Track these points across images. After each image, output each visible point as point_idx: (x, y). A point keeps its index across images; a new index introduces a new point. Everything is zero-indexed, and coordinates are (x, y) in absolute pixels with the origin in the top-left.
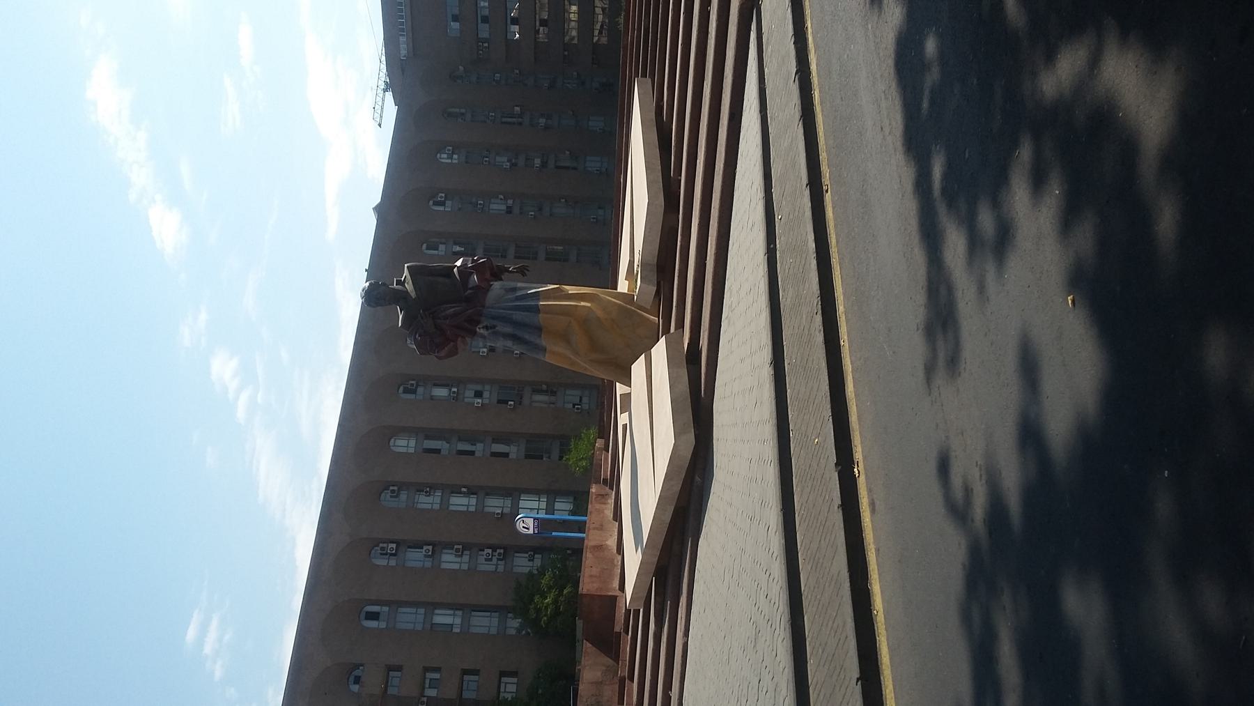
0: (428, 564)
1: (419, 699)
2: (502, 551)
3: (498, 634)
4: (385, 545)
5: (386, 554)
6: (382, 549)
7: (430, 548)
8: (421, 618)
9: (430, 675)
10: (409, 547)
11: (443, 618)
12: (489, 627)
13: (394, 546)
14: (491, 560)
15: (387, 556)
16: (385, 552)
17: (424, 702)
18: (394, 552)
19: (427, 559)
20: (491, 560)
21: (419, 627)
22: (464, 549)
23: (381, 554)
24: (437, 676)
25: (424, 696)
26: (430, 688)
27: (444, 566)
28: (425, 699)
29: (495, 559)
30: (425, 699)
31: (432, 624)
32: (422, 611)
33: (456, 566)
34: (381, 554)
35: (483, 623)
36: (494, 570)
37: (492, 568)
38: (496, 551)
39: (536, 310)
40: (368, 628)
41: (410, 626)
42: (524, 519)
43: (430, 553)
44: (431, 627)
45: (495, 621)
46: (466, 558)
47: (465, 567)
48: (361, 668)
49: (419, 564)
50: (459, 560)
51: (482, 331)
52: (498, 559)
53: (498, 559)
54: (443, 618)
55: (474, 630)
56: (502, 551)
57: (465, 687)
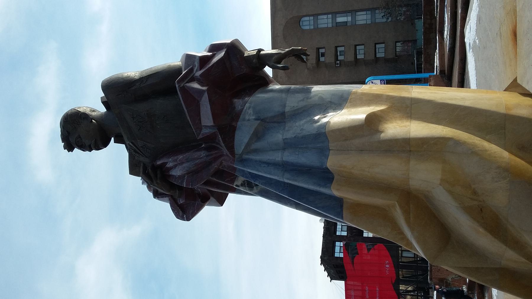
1: (336, 63)
3: (372, 23)
8: (330, 21)
11: (341, 19)
12: (366, 20)
17: (338, 63)
21: (330, 25)
24: (342, 49)
25: (338, 60)
26: (340, 55)
28: (338, 62)
30: (338, 62)
31: (336, 23)
32: (330, 16)
35: (363, 18)
40: (305, 30)
41: (326, 26)
42: (372, 81)
45: (369, 16)
54: (341, 19)
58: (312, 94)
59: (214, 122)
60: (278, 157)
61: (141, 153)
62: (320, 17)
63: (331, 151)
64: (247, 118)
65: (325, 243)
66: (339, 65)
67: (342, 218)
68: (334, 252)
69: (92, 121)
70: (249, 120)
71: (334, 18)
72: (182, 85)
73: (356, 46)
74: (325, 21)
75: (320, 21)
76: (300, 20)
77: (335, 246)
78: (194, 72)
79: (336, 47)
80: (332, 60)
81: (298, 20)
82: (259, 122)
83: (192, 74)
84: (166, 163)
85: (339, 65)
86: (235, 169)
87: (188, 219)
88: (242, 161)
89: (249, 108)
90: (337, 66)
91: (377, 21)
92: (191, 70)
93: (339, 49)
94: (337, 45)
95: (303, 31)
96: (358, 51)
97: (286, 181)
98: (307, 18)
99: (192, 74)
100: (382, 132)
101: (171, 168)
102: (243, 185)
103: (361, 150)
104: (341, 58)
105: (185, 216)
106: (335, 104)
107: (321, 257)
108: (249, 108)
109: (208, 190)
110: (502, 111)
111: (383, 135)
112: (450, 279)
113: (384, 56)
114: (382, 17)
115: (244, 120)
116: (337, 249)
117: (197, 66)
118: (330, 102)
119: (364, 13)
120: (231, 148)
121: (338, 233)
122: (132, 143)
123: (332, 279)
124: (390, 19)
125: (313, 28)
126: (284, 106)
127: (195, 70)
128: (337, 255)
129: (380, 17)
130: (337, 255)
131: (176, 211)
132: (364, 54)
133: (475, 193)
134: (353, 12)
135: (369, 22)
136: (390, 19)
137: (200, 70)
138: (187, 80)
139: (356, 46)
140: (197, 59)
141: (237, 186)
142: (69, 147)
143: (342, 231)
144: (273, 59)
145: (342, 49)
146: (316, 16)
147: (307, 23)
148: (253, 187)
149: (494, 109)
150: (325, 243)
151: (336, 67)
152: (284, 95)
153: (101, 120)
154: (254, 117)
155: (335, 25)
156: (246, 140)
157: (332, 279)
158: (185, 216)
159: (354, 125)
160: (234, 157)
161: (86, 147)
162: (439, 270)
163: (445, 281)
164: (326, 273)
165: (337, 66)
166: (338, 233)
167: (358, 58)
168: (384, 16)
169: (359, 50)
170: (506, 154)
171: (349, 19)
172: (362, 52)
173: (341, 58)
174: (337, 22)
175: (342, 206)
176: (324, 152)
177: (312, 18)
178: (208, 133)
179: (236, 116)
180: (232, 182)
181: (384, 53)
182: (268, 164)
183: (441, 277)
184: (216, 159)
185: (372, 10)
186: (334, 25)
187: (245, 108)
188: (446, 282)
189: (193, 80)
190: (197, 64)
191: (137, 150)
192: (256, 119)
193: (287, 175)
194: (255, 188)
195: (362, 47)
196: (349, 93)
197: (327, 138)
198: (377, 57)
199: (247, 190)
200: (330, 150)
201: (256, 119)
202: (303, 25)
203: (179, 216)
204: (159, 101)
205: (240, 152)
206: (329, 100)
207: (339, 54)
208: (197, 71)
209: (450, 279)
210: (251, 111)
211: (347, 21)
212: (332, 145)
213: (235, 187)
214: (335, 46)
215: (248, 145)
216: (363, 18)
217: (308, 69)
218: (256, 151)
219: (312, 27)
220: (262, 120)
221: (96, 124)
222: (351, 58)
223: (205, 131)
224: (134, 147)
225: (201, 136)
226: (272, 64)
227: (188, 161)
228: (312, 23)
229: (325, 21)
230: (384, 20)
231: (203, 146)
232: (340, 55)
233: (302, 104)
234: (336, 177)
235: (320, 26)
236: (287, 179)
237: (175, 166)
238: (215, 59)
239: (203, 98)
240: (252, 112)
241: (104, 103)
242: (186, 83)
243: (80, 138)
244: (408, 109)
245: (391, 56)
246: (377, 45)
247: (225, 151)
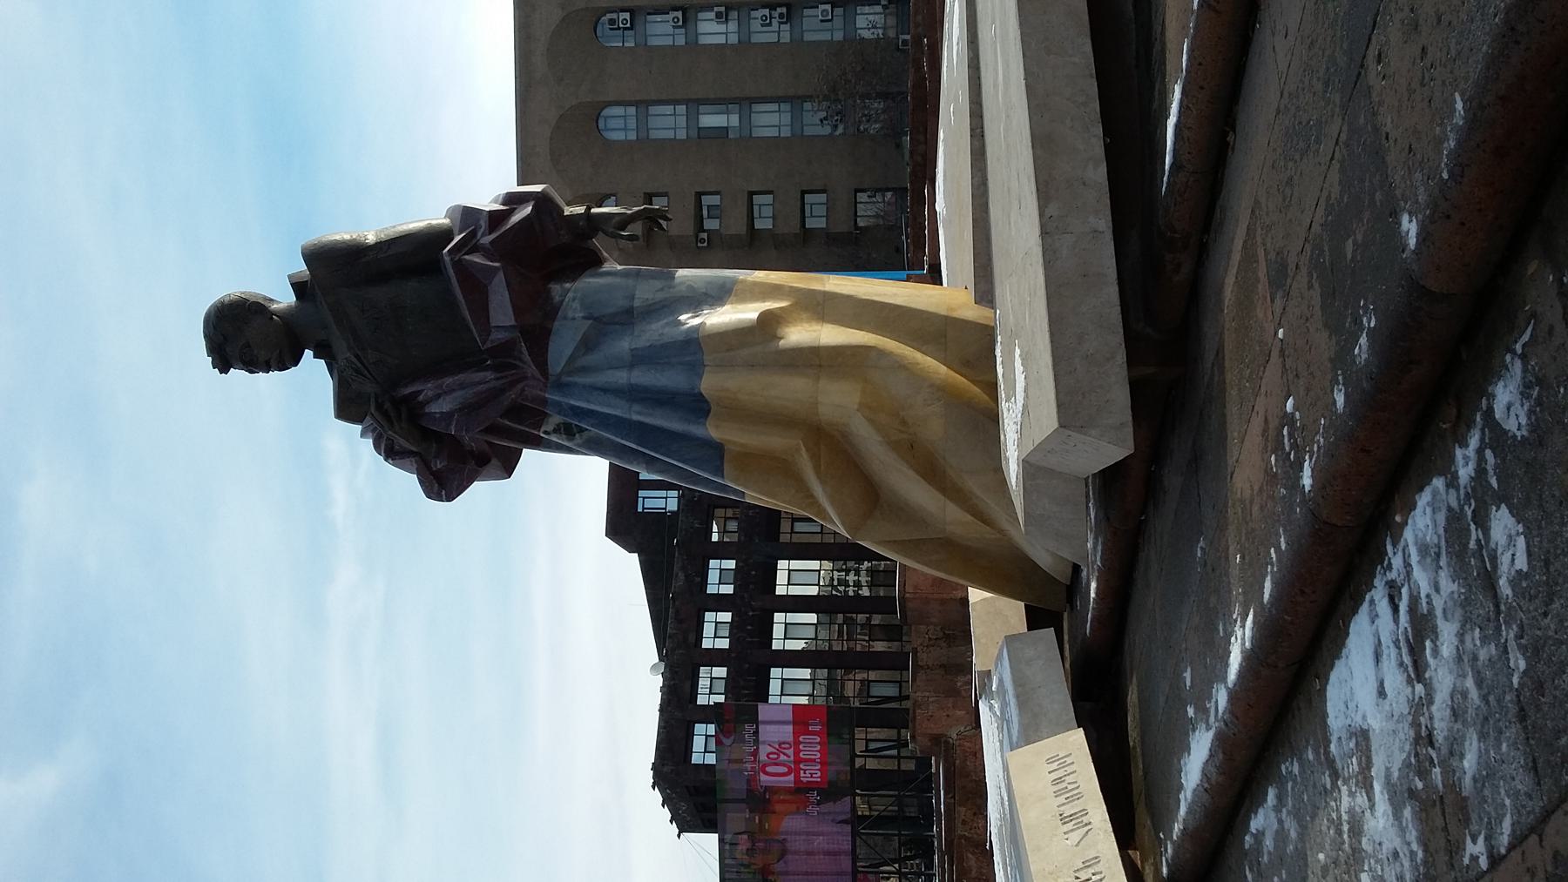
0: (681, 41)
1: (697, 237)
2: (784, 10)
3: (793, 135)
4: (614, 16)
5: (619, 28)
6: (612, 22)
7: (679, 14)
8: (682, 121)
9: (707, 200)
10: (649, 14)
13: (627, 15)
14: (770, 24)
15: (621, 31)
16: (616, 26)
18: (628, 25)
19: (677, 31)
20: (770, 24)
21: (682, 135)
22: (727, 9)
23: (611, 29)
24: (714, 200)
25: (704, 231)
26: (708, 218)
27: (704, 40)
28: (705, 236)
29: (775, 22)
30: (705, 236)
31: (699, 128)
32: (682, 109)
33: (721, 40)
34: (611, 29)
35: (770, 121)
36: (776, 40)
37: (773, 38)
38: (776, 10)
39: (698, 406)
40: (614, 141)
41: (670, 134)
43: (680, 23)
44: (699, 132)
45: (787, 118)
46: (733, 26)
47: (734, 39)
48: (613, 198)
49: (668, 41)
50: (722, 28)
51: (554, 438)
52: (780, 23)
53: (780, 23)
55: (757, 133)
56: (784, 10)
57: (756, 214)
58: (677, 281)
59: (516, 320)
60: (621, 377)
61: (369, 376)
62: (654, 110)
63: (706, 368)
64: (570, 314)
65: (665, 728)
66: (705, 244)
67: (723, 477)
68: (688, 750)
69: (272, 318)
70: (574, 319)
71: (692, 117)
72: (457, 258)
73: (751, 194)
74: (668, 122)
75: (653, 122)
76: (599, 114)
77: (704, 622)
78: (478, 238)
79: (699, 195)
80: (688, 228)
81: (593, 113)
82: (590, 322)
83: (474, 241)
84: (420, 392)
85: (705, 244)
86: (545, 402)
87: (450, 498)
88: (561, 386)
89: (574, 299)
90: (699, 245)
91: (808, 131)
92: (473, 234)
93: (707, 200)
94: (701, 190)
95: (609, 144)
96: (756, 208)
97: (635, 417)
98: (618, 111)
99: (474, 241)
100: (781, 338)
101: (428, 402)
102: (556, 431)
103: (751, 365)
104: (712, 224)
105: (443, 492)
106: (713, 297)
107: (655, 767)
108: (574, 299)
109: (486, 441)
110: (943, 312)
111: (782, 342)
112: (954, 736)
113: (824, 226)
114: (821, 121)
115: (565, 318)
116: (698, 743)
117: (483, 227)
118: (706, 294)
119: (774, 107)
120: (542, 364)
121: (711, 590)
122: (357, 356)
123: (682, 830)
124: (840, 130)
125: (635, 138)
126: (632, 297)
127: (480, 234)
128: (696, 759)
129: (814, 122)
130: (696, 759)
131: (427, 484)
132: (774, 218)
133: (904, 422)
134: (744, 103)
135: (786, 133)
136: (840, 130)
137: (490, 234)
138: (467, 249)
139: (751, 194)
140: (485, 213)
141: (545, 432)
142: (223, 364)
143: (711, 693)
144: (614, 221)
145: (714, 200)
146: (643, 104)
147: (619, 124)
148: (574, 435)
149: (931, 309)
150: (665, 728)
151: (698, 247)
152: (631, 282)
153: (287, 317)
154: (581, 315)
155: (696, 136)
156: (568, 352)
157: (681, 831)
158: (443, 492)
159: (741, 327)
160: (547, 379)
161: (252, 366)
162: (932, 716)
163: (943, 740)
164: (666, 813)
165: (699, 245)
166: (711, 590)
167: (756, 227)
168: (826, 118)
169: (760, 205)
170: (943, 369)
171: (734, 120)
172: (768, 211)
173: (712, 224)
174: (700, 126)
175: (722, 458)
176: (696, 368)
177: (632, 110)
178: (503, 339)
179: (552, 311)
180: (539, 428)
181: (825, 219)
182: (605, 390)
183: (935, 732)
184: (512, 384)
185: (795, 101)
186: (694, 133)
187: (567, 300)
188: (947, 742)
189: (475, 249)
190: (483, 223)
191: (362, 368)
192: (585, 318)
193: (636, 407)
194: (577, 435)
195: (769, 199)
196: (735, 281)
197: (701, 348)
198: (807, 226)
199: (563, 440)
200: (705, 366)
201: (585, 318)
202: (607, 130)
203: (433, 493)
204: (410, 284)
205: (559, 370)
206: (704, 290)
207: (705, 212)
208: (483, 235)
209: (954, 736)
210: (576, 305)
211: (726, 125)
212: (707, 359)
213: (542, 435)
214: (696, 192)
215: (572, 358)
216: (770, 121)
217: (620, 250)
218: (584, 370)
219: (632, 136)
220: (595, 319)
221: (281, 323)
222: (738, 227)
223: (497, 337)
224: (359, 365)
225: (489, 345)
226: (611, 230)
227: (462, 386)
228: (632, 123)
229: (668, 122)
230: (827, 130)
231: (489, 362)
232: (708, 218)
233: (660, 296)
234: (714, 408)
235: (654, 135)
236: (637, 414)
237: (438, 397)
238: (516, 218)
239: (496, 280)
240: (578, 305)
241: (299, 287)
242: (464, 255)
243: (249, 346)
244: (820, 307)
245: (843, 227)
246: (806, 195)
247: (532, 370)
